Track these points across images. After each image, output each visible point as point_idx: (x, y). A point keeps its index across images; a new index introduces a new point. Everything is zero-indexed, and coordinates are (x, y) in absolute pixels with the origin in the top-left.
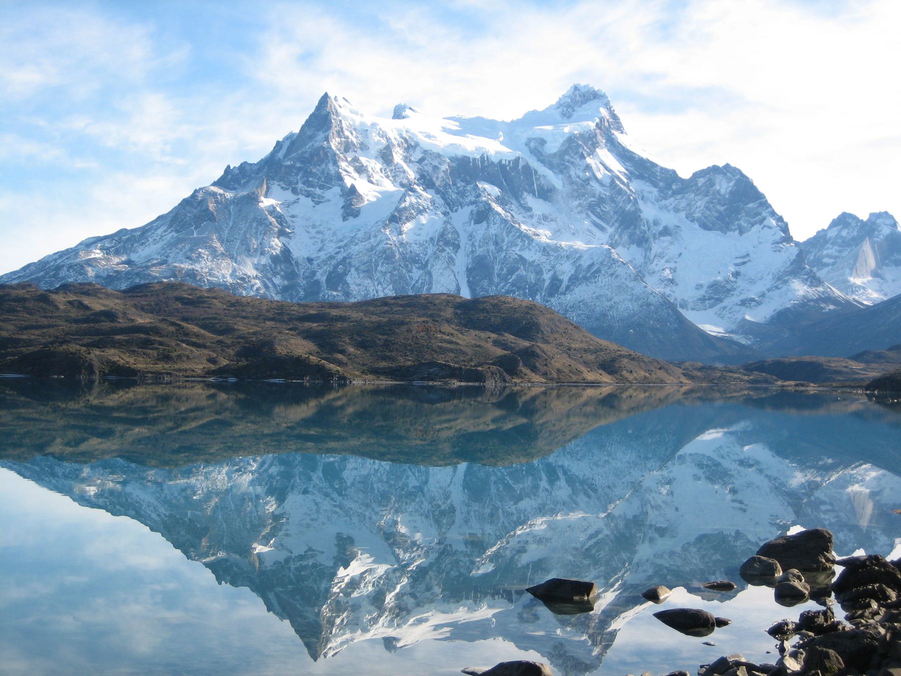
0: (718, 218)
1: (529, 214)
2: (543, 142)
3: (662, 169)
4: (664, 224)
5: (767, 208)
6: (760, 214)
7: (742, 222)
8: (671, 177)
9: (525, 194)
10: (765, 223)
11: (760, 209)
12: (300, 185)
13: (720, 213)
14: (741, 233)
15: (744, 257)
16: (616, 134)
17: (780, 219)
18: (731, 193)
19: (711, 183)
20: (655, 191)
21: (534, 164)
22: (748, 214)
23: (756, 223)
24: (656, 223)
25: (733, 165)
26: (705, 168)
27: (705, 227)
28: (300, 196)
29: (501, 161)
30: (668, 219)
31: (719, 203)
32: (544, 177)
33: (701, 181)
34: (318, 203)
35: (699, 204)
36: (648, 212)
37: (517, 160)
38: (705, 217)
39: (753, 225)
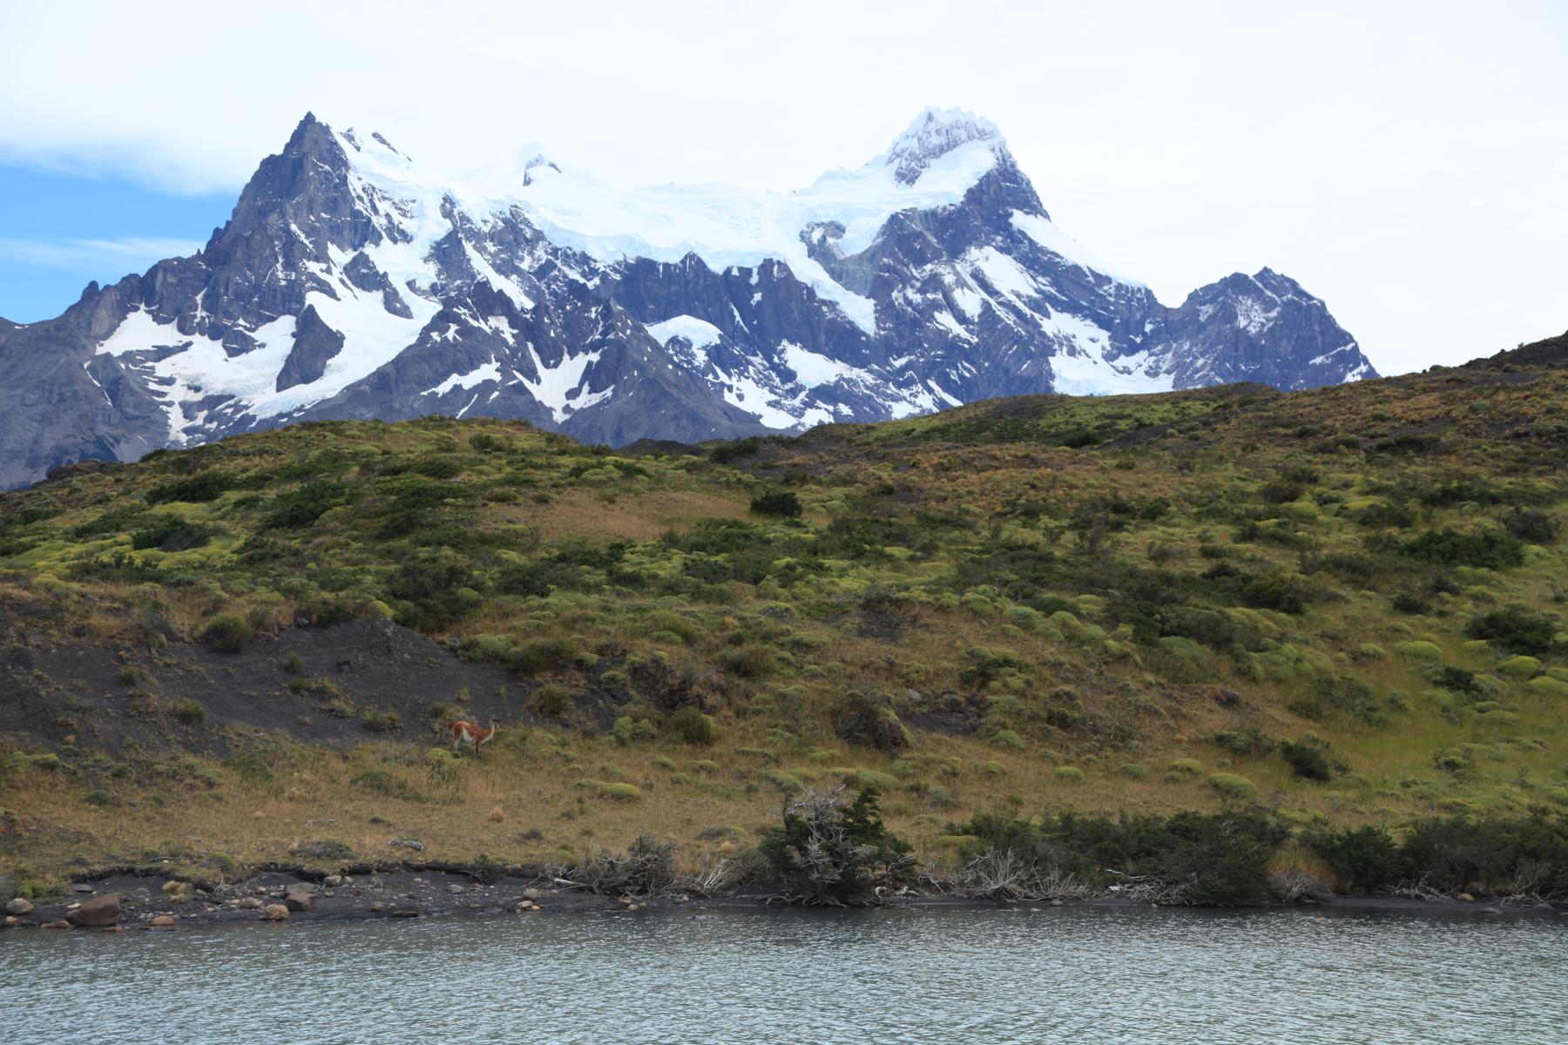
1: (789, 386)
2: (838, 230)
3: (1119, 287)
5: (1357, 365)
8: (1147, 303)
9: (785, 343)
12: (200, 313)
16: (1019, 219)
19: (1227, 315)
20: (1103, 336)
21: (808, 271)
25: (1277, 271)
26: (1216, 280)
28: (196, 338)
29: (729, 270)
32: (832, 305)
33: (1207, 311)
34: (233, 353)
37: (767, 265)
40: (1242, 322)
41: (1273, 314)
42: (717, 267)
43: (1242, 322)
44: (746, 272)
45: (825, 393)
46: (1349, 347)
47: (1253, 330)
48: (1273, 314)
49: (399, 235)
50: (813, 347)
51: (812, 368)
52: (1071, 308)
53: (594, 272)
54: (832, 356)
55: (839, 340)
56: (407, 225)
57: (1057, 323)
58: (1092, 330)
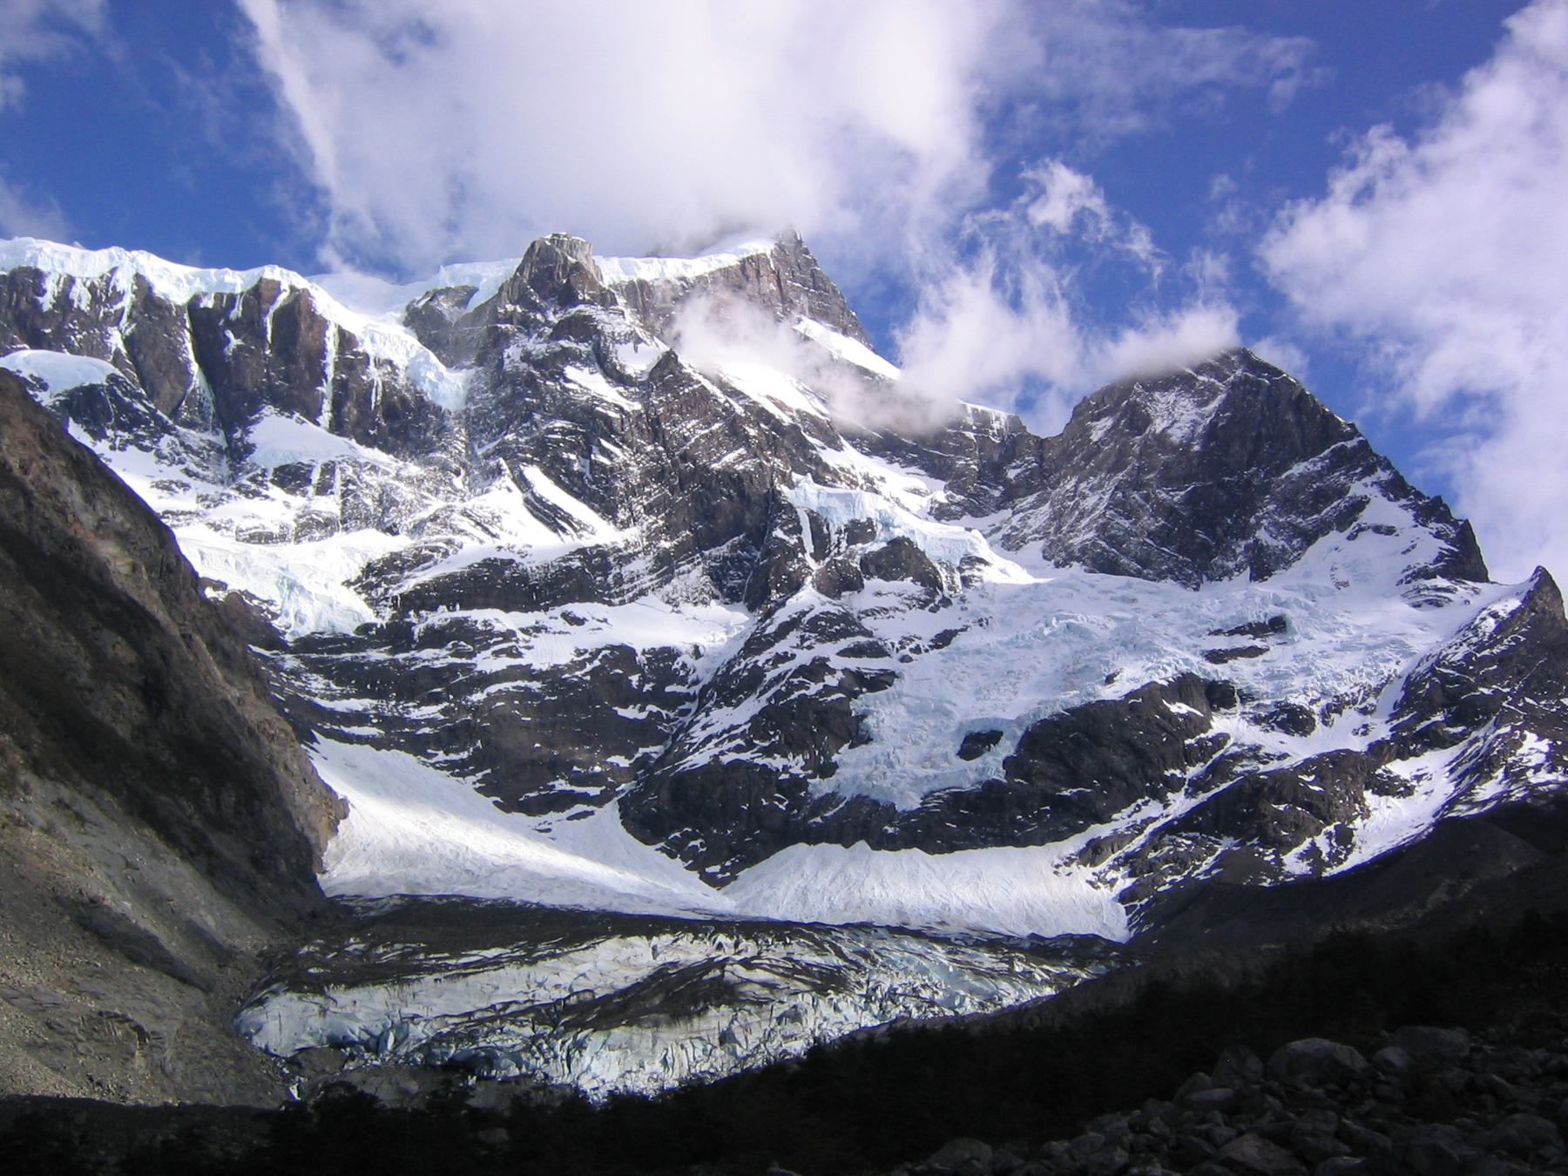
0: (1162, 537)
6: (1341, 492)
7: (1262, 535)
10: (1366, 517)
11: (1339, 477)
13: (1169, 511)
15: (1257, 630)
18: (1212, 432)
19: (1137, 420)
22: (1288, 503)
23: (1322, 529)
31: (1167, 480)
33: (1099, 430)
35: (1091, 501)
38: (1113, 541)
39: (1309, 538)
40: (1159, 426)
41: (1215, 404)
43: (1159, 426)
46: (1350, 444)
47: (1176, 435)
48: (1215, 404)
58: (920, 481)
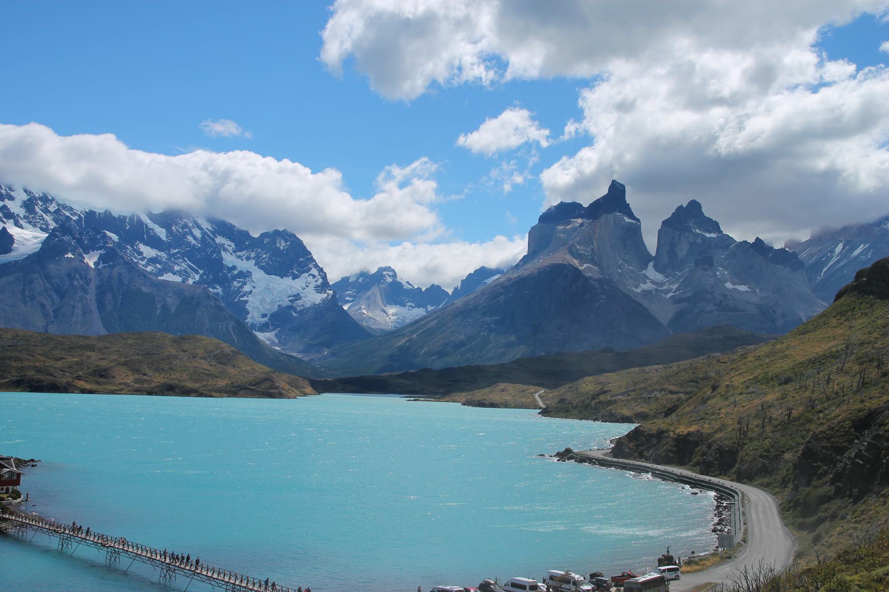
4: (239, 269)
14: (294, 279)
17: (321, 270)
20: (233, 245)
21: (146, 220)
24: (234, 268)
27: (268, 272)
30: (244, 265)
33: (266, 241)
36: (229, 259)
42: (116, 215)
44: (125, 218)
45: (153, 261)
49: (11, 198)
50: (146, 244)
51: (148, 252)
52: (223, 235)
53: (75, 214)
54: (152, 247)
55: (155, 242)
56: (12, 193)
57: (219, 240)
